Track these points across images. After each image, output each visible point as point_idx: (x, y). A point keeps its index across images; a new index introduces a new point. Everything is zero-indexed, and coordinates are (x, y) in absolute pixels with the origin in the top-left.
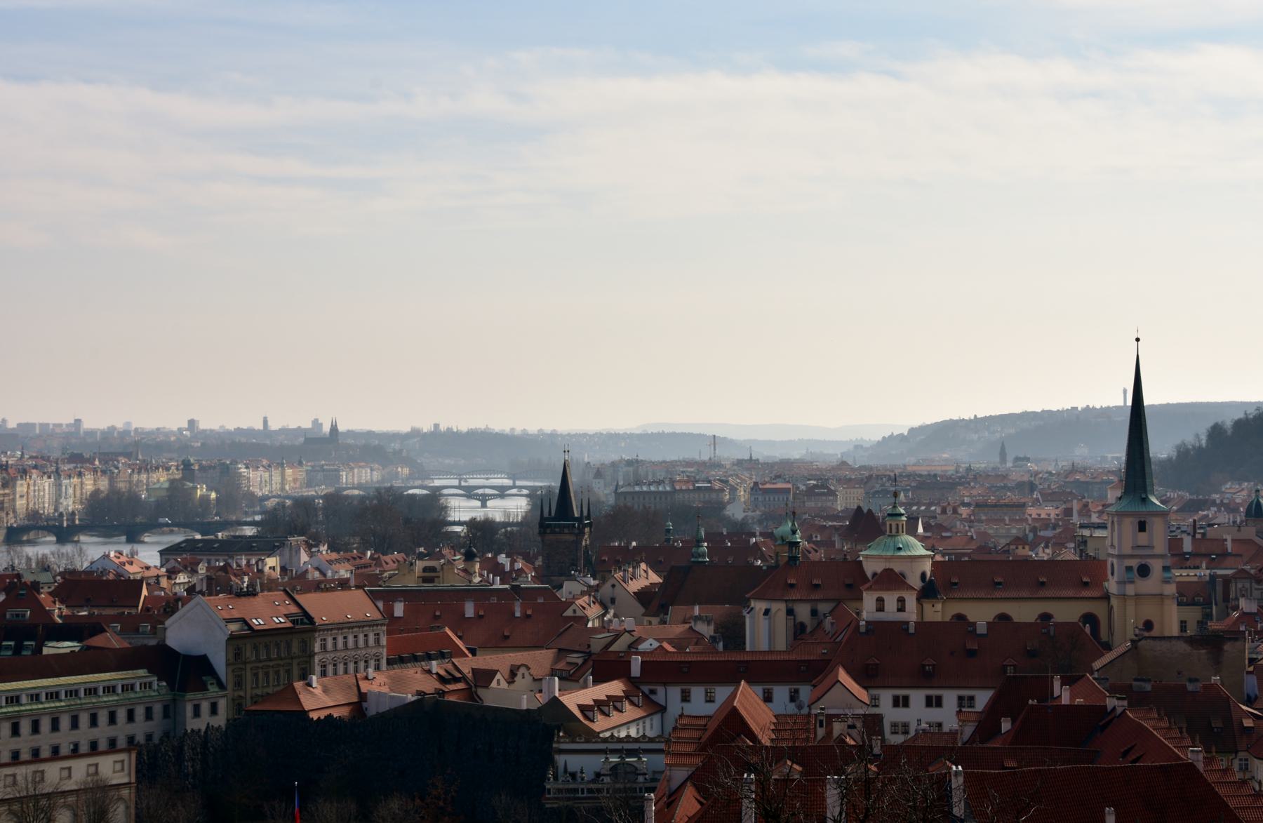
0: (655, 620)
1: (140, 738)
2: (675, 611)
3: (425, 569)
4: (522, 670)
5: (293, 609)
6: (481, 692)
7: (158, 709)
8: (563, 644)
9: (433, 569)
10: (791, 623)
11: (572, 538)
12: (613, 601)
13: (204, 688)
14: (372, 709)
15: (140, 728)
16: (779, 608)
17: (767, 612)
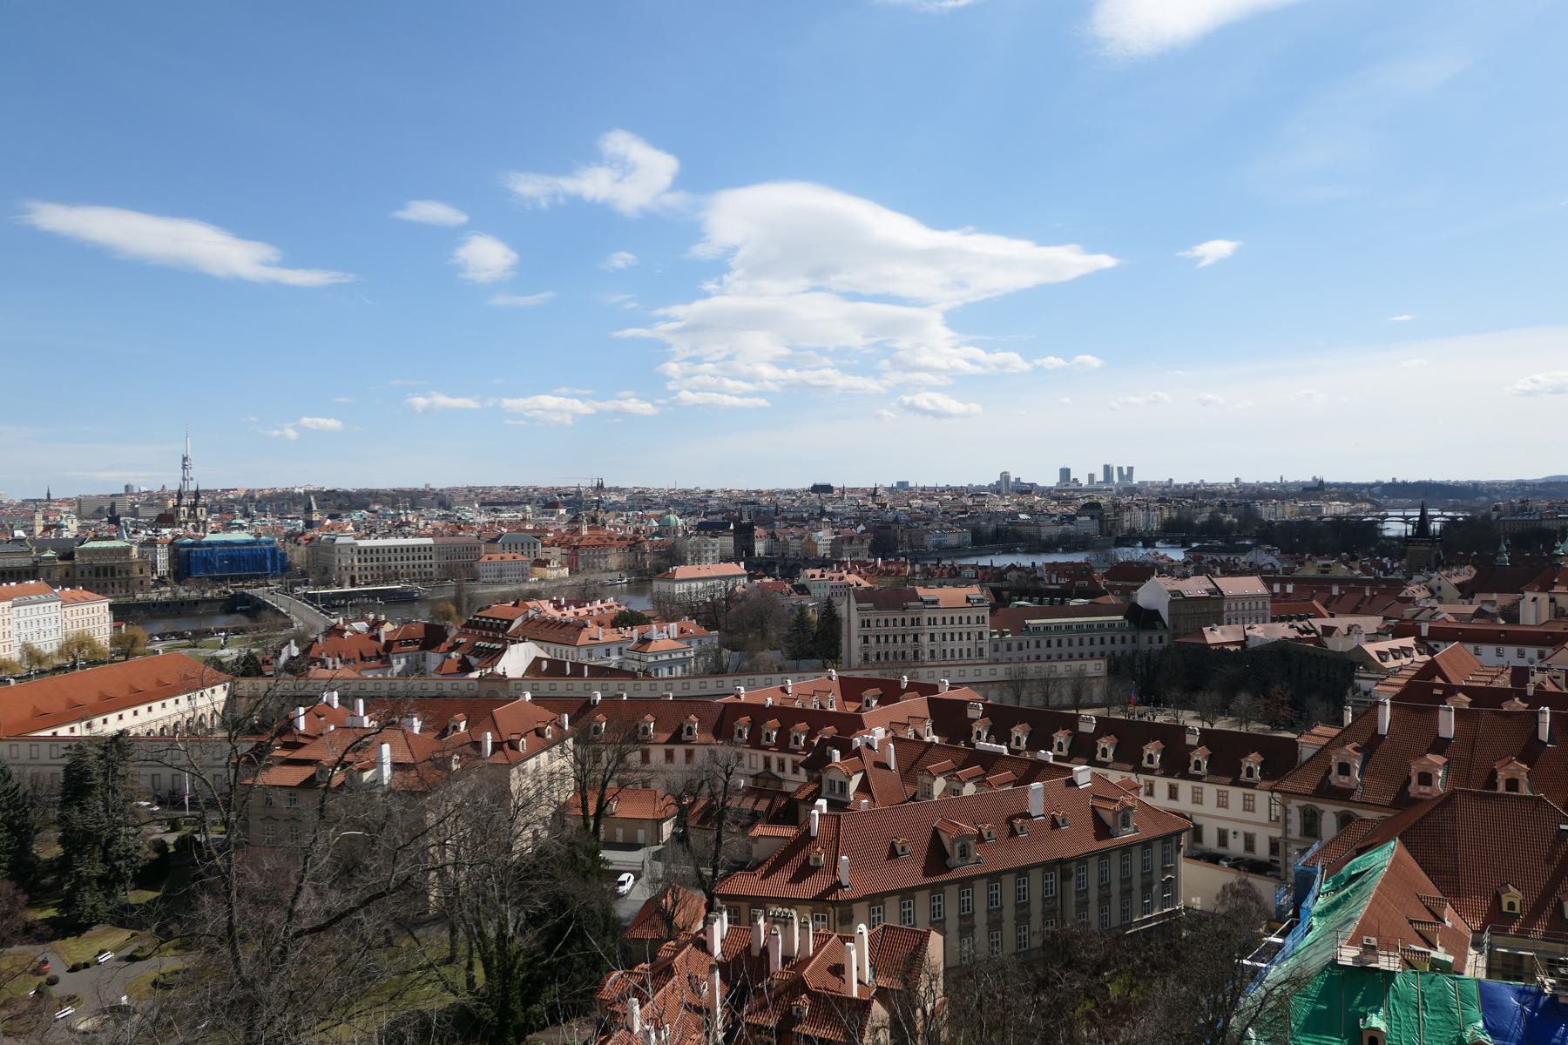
0: (1466, 601)
1: (1118, 654)
2: (1478, 597)
3: (1324, 566)
4: (1355, 628)
5: (1212, 586)
6: (1326, 639)
7: (1129, 637)
8: (1387, 613)
9: (1328, 566)
10: (1553, 607)
11: (1427, 549)
12: (1439, 588)
13: (1156, 628)
14: (1251, 644)
15: (1118, 648)
16: (1544, 598)
17: (1534, 600)
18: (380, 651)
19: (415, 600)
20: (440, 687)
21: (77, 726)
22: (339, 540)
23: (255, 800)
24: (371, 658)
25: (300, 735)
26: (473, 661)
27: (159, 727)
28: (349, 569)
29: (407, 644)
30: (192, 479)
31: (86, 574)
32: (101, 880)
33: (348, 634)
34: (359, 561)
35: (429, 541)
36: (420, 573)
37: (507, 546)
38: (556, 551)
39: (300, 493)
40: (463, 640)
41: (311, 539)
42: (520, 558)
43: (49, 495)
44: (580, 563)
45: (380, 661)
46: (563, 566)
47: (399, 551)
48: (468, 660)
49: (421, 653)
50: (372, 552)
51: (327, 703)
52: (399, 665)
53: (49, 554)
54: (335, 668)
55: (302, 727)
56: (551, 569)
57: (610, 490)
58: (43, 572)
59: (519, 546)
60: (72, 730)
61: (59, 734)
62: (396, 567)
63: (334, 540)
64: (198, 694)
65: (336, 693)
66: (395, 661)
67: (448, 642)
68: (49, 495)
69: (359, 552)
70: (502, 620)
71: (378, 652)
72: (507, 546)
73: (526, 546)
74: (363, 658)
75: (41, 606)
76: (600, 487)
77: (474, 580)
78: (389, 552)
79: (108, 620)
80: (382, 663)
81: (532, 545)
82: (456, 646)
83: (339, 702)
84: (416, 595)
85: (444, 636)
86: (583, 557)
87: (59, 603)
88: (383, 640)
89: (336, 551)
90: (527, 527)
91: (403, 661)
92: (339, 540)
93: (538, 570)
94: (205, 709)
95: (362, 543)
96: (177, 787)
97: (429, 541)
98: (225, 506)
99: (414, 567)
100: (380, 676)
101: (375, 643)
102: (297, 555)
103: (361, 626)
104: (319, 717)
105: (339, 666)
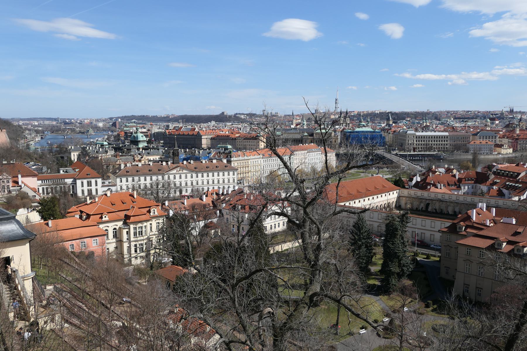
18: (456, 182)
19: (441, 159)
20: (497, 202)
21: (351, 202)
22: (409, 132)
23: (462, 251)
24: (452, 185)
25: (474, 222)
26: (505, 191)
27: (376, 206)
28: (412, 144)
29: (468, 180)
30: (338, 108)
31: (318, 141)
32: (398, 274)
33: (438, 173)
34: (416, 141)
35: (446, 134)
36: (444, 148)
37: (482, 137)
38: (505, 141)
39: (378, 113)
40: (498, 181)
41: (394, 132)
42: (489, 143)
43: (293, 113)
44: (519, 146)
45: (456, 186)
46: (510, 148)
47: (443, 137)
48: (501, 191)
49: (475, 185)
50: (434, 137)
51: (480, 208)
52: (465, 189)
53: (306, 134)
54: (441, 188)
55: (474, 219)
56: (504, 149)
57: (516, 112)
58: (304, 140)
59: (488, 137)
60: (350, 203)
61: (346, 205)
62: (432, 145)
63: (407, 132)
64: (388, 194)
65: (485, 204)
66: (462, 187)
67: (490, 181)
68: (293, 113)
69: (417, 137)
70: (514, 172)
71: (455, 183)
72: (482, 137)
73: (491, 137)
74: (449, 185)
75: (315, 153)
76: (512, 111)
77: (466, 152)
78: (429, 138)
79: (335, 159)
80: (457, 188)
81: (494, 137)
82: (495, 183)
83: (486, 209)
84: (442, 157)
85: (488, 178)
86: (520, 144)
87: (321, 152)
88: (457, 177)
89: (407, 137)
90: (487, 129)
91: (466, 187)
92: (409, 132)
93: (498, 149)
94: (390, 200)
95: (418, 134)
96: (423, 238)
97: (446, 134)
98: (360, 118)
99: (442, 145)
100: (456, 193)
101: (454, 178)
102: (389, 138)
103: (442, 170)
104: (479, 214)
105: (442, 188)
